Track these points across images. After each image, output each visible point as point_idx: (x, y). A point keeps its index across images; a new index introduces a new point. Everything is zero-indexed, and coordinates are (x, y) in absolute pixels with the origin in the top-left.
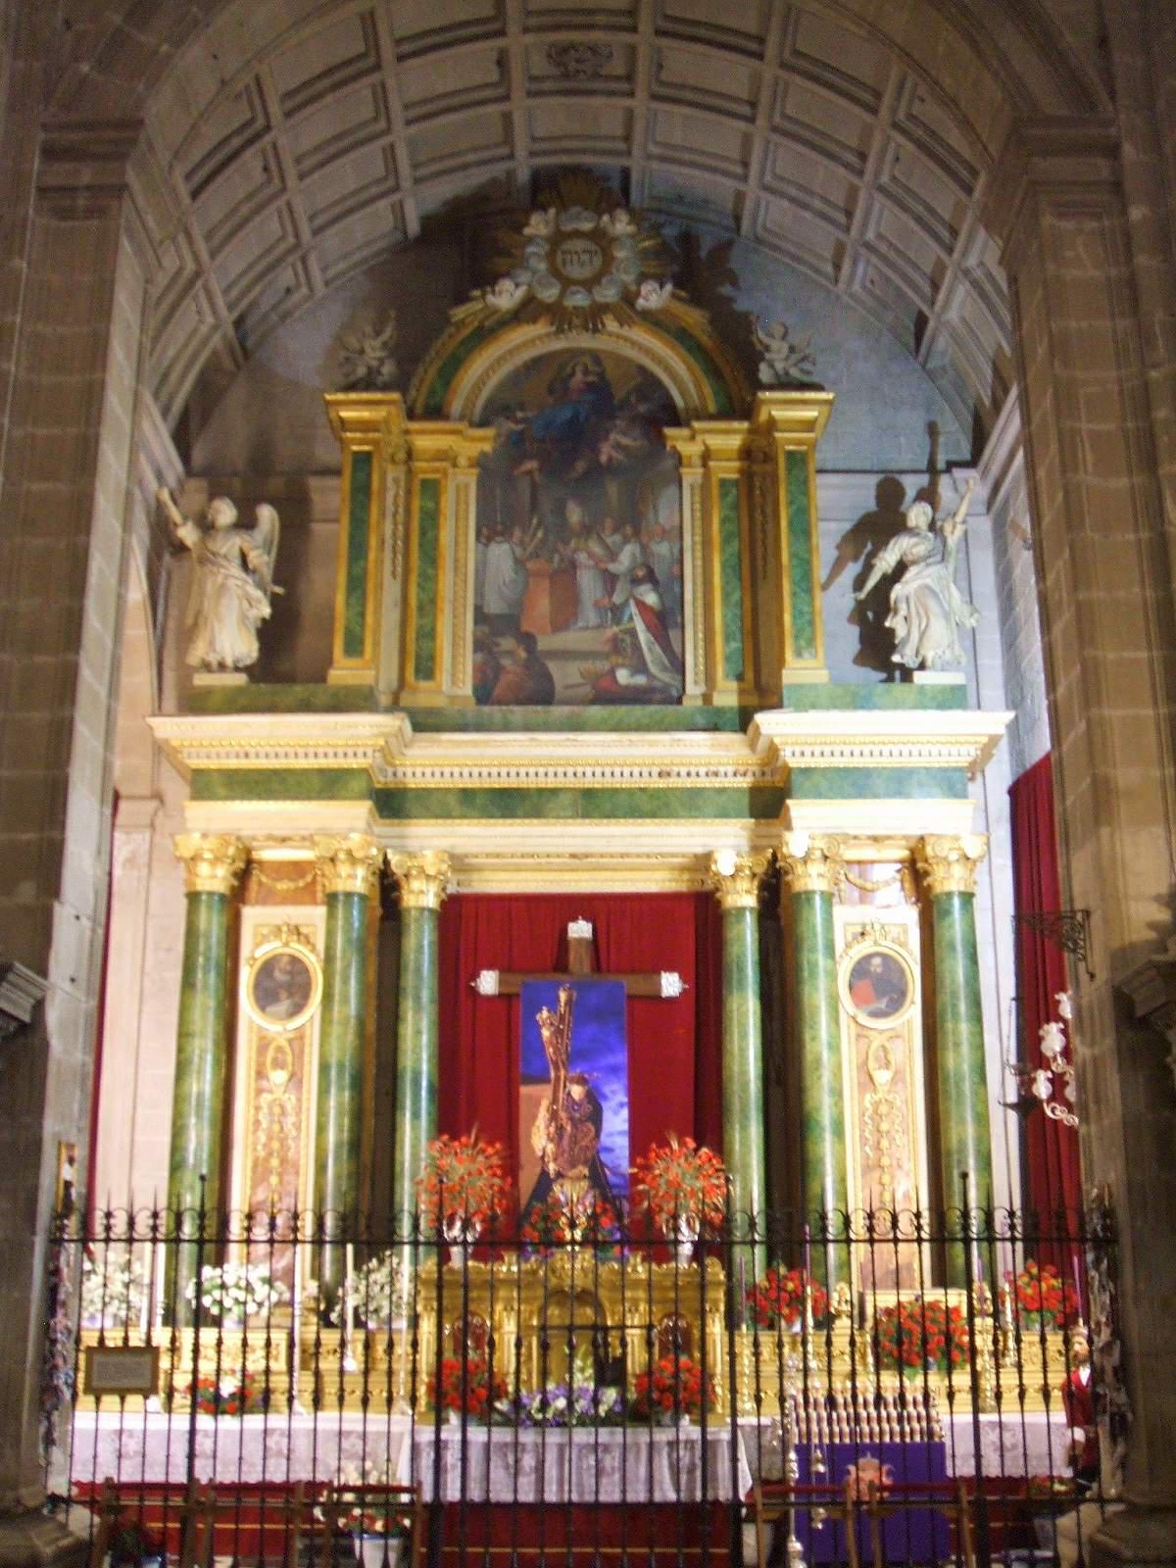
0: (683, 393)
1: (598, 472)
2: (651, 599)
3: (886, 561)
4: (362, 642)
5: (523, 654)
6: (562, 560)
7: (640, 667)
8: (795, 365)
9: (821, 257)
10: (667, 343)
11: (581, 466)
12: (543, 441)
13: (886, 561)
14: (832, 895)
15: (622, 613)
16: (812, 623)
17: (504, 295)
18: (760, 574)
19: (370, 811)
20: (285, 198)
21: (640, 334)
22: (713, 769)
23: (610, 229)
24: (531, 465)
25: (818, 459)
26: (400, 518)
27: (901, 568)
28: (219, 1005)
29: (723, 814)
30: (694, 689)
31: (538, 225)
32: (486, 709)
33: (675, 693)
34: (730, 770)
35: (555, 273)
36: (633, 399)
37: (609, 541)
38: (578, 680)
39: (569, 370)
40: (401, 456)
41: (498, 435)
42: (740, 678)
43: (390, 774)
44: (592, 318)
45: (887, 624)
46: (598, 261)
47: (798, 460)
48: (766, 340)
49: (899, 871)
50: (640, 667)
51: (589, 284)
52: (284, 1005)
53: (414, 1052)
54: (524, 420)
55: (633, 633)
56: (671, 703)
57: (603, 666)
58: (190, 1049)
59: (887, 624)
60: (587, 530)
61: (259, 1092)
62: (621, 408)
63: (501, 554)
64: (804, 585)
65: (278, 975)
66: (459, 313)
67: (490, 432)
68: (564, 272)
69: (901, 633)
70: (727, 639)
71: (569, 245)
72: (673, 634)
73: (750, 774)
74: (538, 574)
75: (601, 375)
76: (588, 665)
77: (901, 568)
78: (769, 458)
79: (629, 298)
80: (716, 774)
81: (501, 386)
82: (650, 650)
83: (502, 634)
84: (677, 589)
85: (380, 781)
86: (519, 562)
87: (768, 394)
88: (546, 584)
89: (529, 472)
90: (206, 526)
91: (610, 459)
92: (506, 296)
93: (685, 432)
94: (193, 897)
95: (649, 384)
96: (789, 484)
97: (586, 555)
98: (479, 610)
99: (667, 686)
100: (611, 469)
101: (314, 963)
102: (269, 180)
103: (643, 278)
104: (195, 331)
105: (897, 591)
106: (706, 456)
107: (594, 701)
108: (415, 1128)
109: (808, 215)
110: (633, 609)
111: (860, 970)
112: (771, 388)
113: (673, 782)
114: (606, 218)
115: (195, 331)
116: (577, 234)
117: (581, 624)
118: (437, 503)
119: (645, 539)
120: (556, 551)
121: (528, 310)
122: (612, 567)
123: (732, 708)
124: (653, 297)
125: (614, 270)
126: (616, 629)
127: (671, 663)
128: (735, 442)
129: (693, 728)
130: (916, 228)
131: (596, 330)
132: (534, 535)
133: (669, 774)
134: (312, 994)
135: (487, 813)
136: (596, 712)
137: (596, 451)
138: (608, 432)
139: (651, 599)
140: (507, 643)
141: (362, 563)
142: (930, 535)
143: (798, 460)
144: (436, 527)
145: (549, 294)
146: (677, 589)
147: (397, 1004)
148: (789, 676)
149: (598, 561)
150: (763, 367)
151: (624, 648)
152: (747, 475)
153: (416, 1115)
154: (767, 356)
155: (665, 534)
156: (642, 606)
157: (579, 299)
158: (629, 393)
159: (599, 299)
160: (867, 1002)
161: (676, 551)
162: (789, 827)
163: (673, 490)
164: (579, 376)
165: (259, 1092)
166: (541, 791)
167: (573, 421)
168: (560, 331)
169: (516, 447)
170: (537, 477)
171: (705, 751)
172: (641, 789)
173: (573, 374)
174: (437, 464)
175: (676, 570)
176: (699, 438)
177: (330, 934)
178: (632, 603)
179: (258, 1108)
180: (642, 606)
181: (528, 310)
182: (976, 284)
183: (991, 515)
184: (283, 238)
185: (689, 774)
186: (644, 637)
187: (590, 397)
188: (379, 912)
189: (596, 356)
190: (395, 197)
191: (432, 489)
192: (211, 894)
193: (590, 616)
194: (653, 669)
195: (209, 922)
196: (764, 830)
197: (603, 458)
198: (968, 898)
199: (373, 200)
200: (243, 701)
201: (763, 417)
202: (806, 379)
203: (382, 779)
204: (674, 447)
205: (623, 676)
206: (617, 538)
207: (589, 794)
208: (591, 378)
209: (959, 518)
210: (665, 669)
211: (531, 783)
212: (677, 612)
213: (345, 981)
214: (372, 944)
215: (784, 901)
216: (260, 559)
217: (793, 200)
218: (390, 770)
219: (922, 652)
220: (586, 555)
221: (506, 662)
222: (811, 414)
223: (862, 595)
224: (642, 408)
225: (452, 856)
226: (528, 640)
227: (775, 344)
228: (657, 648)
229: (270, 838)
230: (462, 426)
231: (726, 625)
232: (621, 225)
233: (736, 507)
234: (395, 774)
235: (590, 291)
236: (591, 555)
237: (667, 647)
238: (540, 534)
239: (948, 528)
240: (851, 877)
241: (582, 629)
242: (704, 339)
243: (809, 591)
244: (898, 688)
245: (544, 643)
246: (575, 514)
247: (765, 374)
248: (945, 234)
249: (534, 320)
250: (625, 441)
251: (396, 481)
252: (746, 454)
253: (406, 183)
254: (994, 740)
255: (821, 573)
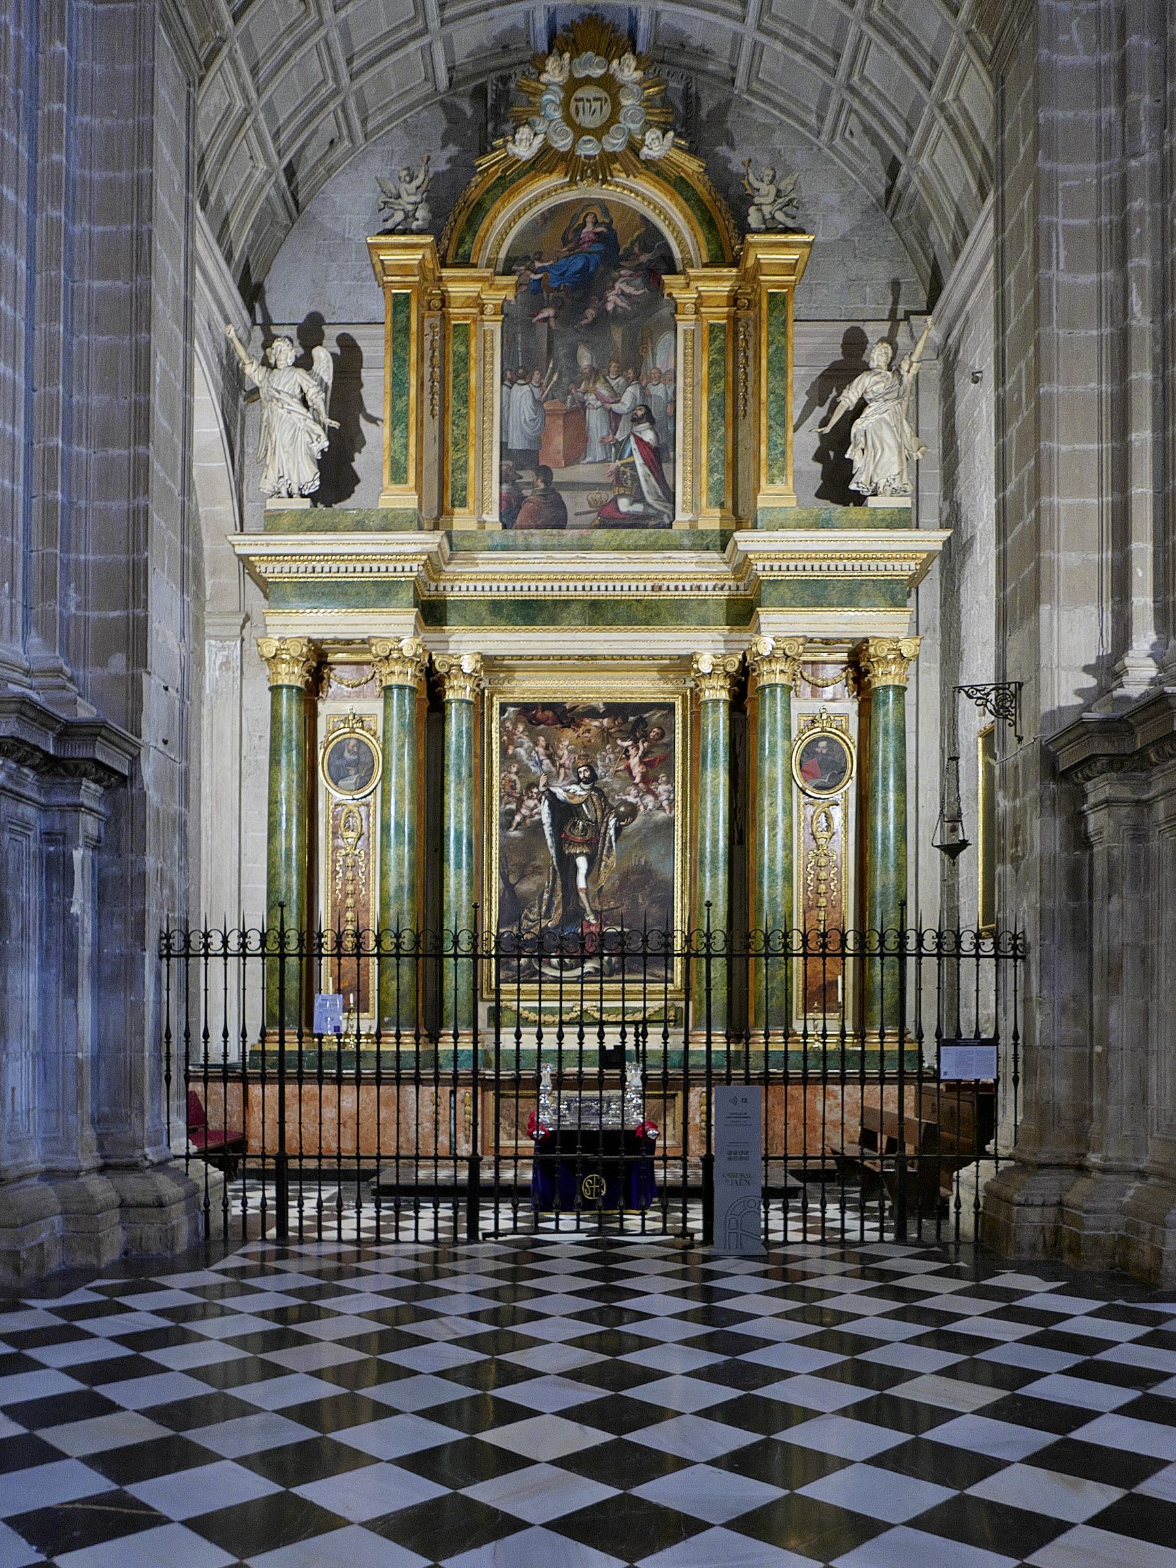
0: (681, 243)
1: (604, 319)
2: (648, 436)
3: (849, 398)
4: (406, 471)
5: (542, 486)
6: (573, 400)
7: (639, 498)
8: (780, 209)
9: (806, 108)
10: (667, 192)
11: (590, 313)
12: (558, 289)
13: (849, 398)
14: (791, 688)
15: (624, 450)
16: (783, 453)
17: (523, 144)
18: (741, 413)
19: (417, 617)
20: (322, 33)
21: (643, 185)
22: (696, 583)
23: (619, 76)
24: (548, 312)
25: (792, 310)
26: (436, 361)
27: (862, 405)
28: (301, 779)
29: (704, 622)
30: (682, 517)
31: (554, 72)
32: (511, 532)
33: (667, 521)
34: (711, 584)
35: (568, 119)
36: (636, 250)
37: (613, 383)
38: (588, 509)
39: (581, 221)
40: (437, 303)
41: (518, 285)
42: (722, 506)
43: (433, 588)
44: (600, 169)
45: (847, 456)
46: (607, 109)
47: (778, 302)
48: (756, 184)
49: (844, 670)
50: (639, 498)
51: (599, 133)
52: (352, 780)
53: (456, 816)
54: (542, 270)
55: (632, 466)
56: (664, 527)
57: (607, 496)
58: (278, 813)
59: (847, 456)
60: (595, 373)
61: (336, 849)
62: (625, 258)
63: (522, 395)
64: (779, 419)
65: (346, 754)
66: (485, 161)
67: (511, 280)
68: (577, 121)
69: (858, 464)
70: (711, 471)
71: (579, 94)
72: (665, 467)
73: (726, 588)
74: (553, 413)
75: (609, 226)
76: (594, 495)
77: (862, 405)
78: (753, 304)
79: (634, 147)
80: (699, 588)
81: (522, 234)
82: (646, 480)
83: (522, 469)
84: (670, 428)
85: (426, 595)
86: (537, 403)
87: (757, 238)
88: (561, 422)
89: (546, 319)
90: (268, 364)
91: (616, 306)
92: (524, 146)
93: (681, 279)
94: (275, 690)
95: (651, 236)
96: (770, 325)
97: (594, 396)
98: (503, 445)
99: (660, 514)
100: (616, 317)
101: (376, 747)
102: (306, 12)
103: (648, 125)
104: (250, 176)
105: (858, 426)
106: (699, 302)
107: (599, 527)
108: (458, 875)
109: (799, 58)
110: (633, 444)
111: (810, 749)
112: (757, 232)
113: (663, 595)
114: (615, 63)
115: (250, 176)
116: (588, 80)
117: (589, 459)
118: (467, 347)
119: (644, 384)
120: (569, 393)
121: (545, 160)
122: (615, 407)
123: (714, 531)
124: (656, 146)
125: (621, 119)
126: (618, 463)
127: (664, 493)
128: (724, 288)
129: (679, 548)
130: (901, 63)
131: (604, 181)
132: (550, 378)
133: (660, 589)
134: (375, 770)
135: (511, 620)
136: (601, 535)
137: (603, 299)
138: (615, 281)
139: (648, 436)
140: (528, 476)
141: (405, 398)
142: (889, 373)
143: (778, 302)
144: (467, 370)
145: (562, 144)
146: (670, 428)
147: (443, 777)
148: (762, 502)
149: (604, 402)
150: (752, 210)
151: (624, 480)
152: (734, 320)
153: (458, 865)
154: (757, 200)
155: (660, 378)
156: (639, 441)
157: (588, 148)
158: (632, 244)
159: (609, 148)
160: (814, 776)
161: (670, 392)
162: (758, 632)
163: (669, 336)
164: (589, 227)
165: (336, 849)
166: (556, 603)
167: (584, 270)
168: (573, 182)
169: (534, 294)
170: (552, 323)
171: (692, 567)
172: (637, 601)
173: (584, 225)
174: (468, 310)
175: (670, 410)
176: (693, 284)
177: (386, 719)
178: (632, 439)
179: (335, 861)
180: (639, 441)
181: (545, 160)
182: (950, 120)
183: (941, 357)
184: (324, 81)
185: (676, 588)
186: (642, 470)
187: (598, 247)
188: (426, 705)
189: (603, 205)
190: (426, 40)
191: (463, 333)
192: (290, 687)
193: (596, 451)
194: (649, 499)
195: (290, 710)
196: (736, 636)
197: (610, 307)
198: (901, 691)
199: (403, 44)
200: (309, 522)
201: (750, 262)
202: (791, 224)
203: (427, 593)
204: (670, 295)
205: (624, 505)
206: (621, 380)
207: (595, 604)
208: (599, 229)
209: (914, 358)
210: (658, 499)
211: (548, 595)
212: (671, 449)
213: (400, 758)
214: (422, 728)
215: (750, 694)
216: (317, 398)
217: (786, 42)
218: (433, 585)
219: (875, 480)
220: (594, 396)
221: (526, 492)
222: (791, 256)
223: (827, 430)
224: (644, 258)
225: (484, 658)
226: (545, 473)
227: (764, 188)
228: (652, 479)
229: (336, 641)
230: (487, 273)
231: (709, 459)
232: (628, 71)
233: (722, 351)
234: (437, 589)
235: (600, 141)
236: (599, 397)
237: (661, 479)
238: (555, 378)
239: (905, 366)
240: (805, 674)
241: (589, 463)
242: (701, 190)
243: (783, 425)
244: (853, 511)
245: (559, 475)
246: (585, 359)
247: (754, 219)
248: (926, 67)
249: (551, 172)
250: (629, 290)
251: (432, 327)
252: (733, 299)
253: (434, 25)
254: (931, 555)
255: (794, 410)
